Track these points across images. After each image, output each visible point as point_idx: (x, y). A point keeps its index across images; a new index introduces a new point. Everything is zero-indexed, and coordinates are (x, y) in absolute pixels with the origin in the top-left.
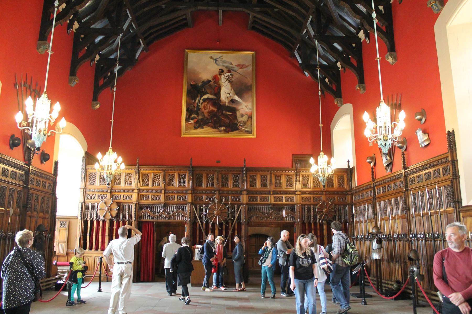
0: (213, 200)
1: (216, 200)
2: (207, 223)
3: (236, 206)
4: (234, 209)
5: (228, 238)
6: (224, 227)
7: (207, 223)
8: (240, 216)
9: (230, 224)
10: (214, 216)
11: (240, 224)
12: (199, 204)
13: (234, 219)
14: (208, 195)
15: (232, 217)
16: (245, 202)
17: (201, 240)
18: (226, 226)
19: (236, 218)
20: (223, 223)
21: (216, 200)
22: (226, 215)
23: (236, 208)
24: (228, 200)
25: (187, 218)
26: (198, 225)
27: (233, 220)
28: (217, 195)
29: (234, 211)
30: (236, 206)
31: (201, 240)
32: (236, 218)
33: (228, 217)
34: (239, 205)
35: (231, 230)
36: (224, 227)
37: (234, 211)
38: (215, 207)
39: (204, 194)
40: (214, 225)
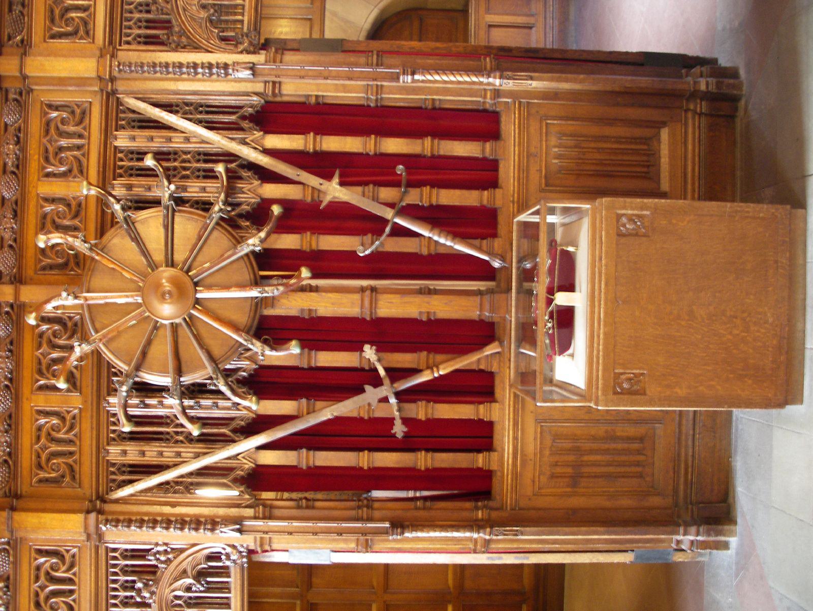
0: (73, 328)
1: (64, 302)
2: (262, 382)
3: (123, 140)
4: (140, 155)
5: (388, 214)
6: (288, 241)
7: (262, 382)
8: (208, 114)
9: (271, 190)
10: (191, 322)
11: (272, 115)
12: (99, 450)
13: (228, 157)
14: (28, 372)
15: (210, 175)
16: (86, 67)
17: (399, 429)
18: (284, 226)
19: (218, 141)
20: (254, 243)
21: (64, 302)
22: (186, 226)
23: (140, 140)
24: (77, 208)
25: (217, 547)
26: (271, 458)
27: (241, 169)
28: (29, 294)
29: (160, 156)
30: (123, 140)
31: (399, 429)
32: (218, 141)
33: (205, 206)
34: (118, 116)
35: (313, 181)
36: (288, 241)
37: (160, 156)
38: (126, 309)
39: (17, 399)
40: (271, 330)
